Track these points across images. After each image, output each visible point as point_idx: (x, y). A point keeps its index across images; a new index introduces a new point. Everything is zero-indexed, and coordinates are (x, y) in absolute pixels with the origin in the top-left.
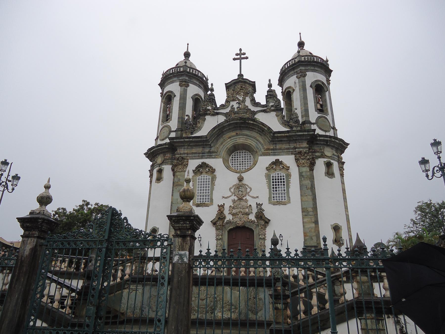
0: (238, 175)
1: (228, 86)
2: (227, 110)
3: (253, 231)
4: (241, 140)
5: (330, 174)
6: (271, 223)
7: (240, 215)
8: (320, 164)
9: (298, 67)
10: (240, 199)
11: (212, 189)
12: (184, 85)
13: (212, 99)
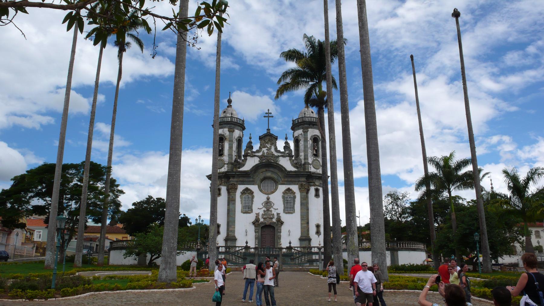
0: (266, 196)
1: (261, 138)
2: (260, 154)
3: (274, 228)
4: (269, 174)
5: (317, 195)
6: (284, 224)
7: (268, 219)
8: (312, 190)
9: (304, 124)
10: (268, 210)
11: (252, 204)
12: (231, 131)
13: (250, 146)
